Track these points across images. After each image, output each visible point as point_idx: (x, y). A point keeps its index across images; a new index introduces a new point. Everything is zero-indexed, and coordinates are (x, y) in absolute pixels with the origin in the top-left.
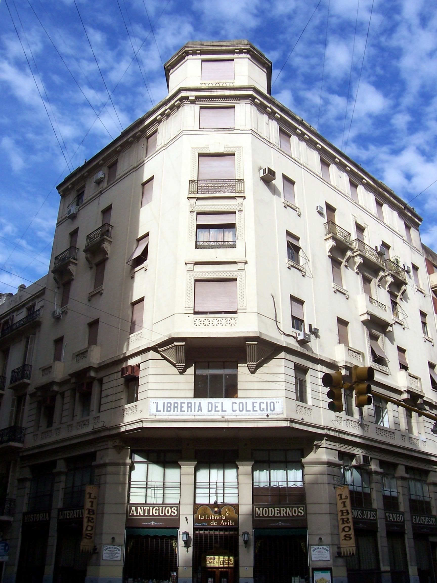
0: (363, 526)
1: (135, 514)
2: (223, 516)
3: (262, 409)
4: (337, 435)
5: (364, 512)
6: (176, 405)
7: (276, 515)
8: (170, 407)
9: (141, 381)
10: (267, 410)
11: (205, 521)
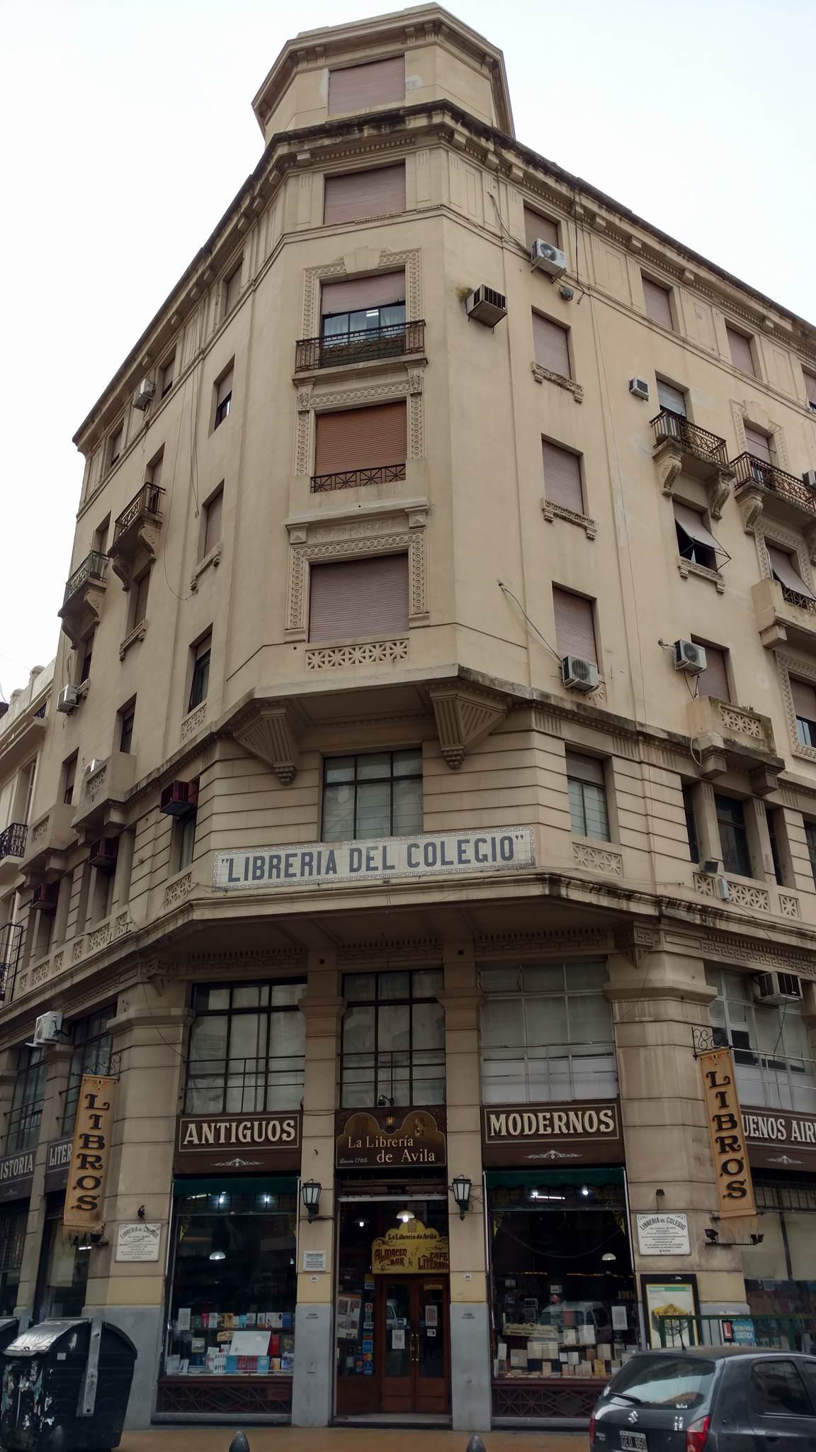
1: (196, 1142)
3: (481, 857)
5: (794, 1123)
6: (275, 861)
7: (541, 1131)
8: (261, 868)
9: (201, 815)
10: (494, 859)
11: (363, 1152)
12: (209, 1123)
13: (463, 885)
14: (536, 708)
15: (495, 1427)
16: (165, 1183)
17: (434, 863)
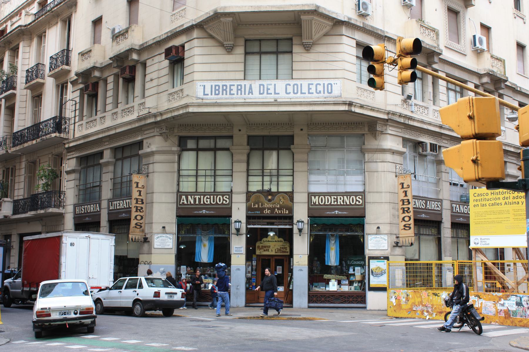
0: (425, 216)
1: (186, 203)
3: (318, 92)
4: (402, 120)
5: (428, 202)
6: (225, 88)
7: (333, 203)
8: (218, 90)
9: (187, 63)
10: (324, 93)
11: (258, 209)
12: (191, 196)
13: (311, 104)
14: (346, 24)
15: (309, 307)
16: (174, 220)
17: (297, 93)
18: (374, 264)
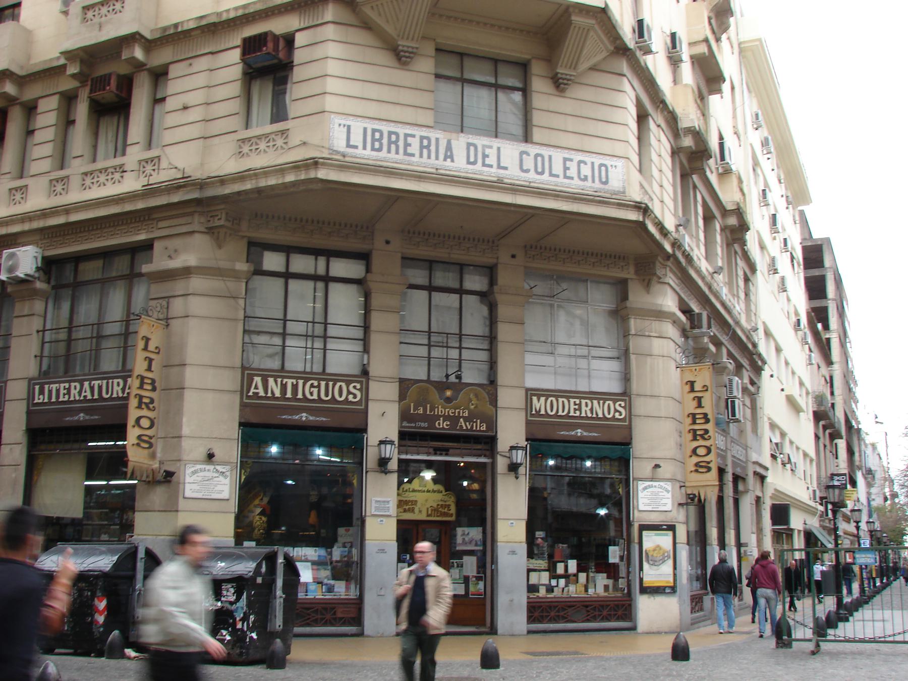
1: (262, 394)
2: (463, 409)
3: (582, 177)
7: (572, 414)
9: (298, 73)
10: (593, 181)
11: (424, 417)
12: (275, 378)
13: (576, 199)
15: (530, 632)
16: (234, 432)
18: (651, 540)
